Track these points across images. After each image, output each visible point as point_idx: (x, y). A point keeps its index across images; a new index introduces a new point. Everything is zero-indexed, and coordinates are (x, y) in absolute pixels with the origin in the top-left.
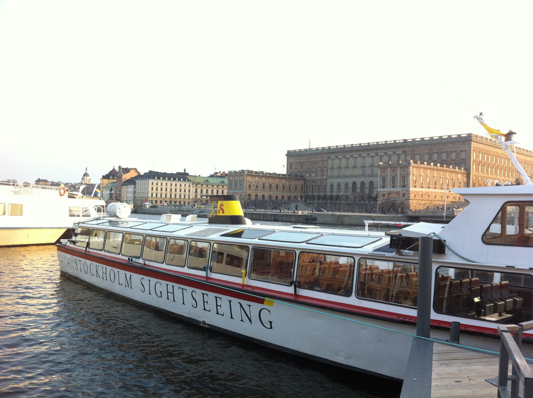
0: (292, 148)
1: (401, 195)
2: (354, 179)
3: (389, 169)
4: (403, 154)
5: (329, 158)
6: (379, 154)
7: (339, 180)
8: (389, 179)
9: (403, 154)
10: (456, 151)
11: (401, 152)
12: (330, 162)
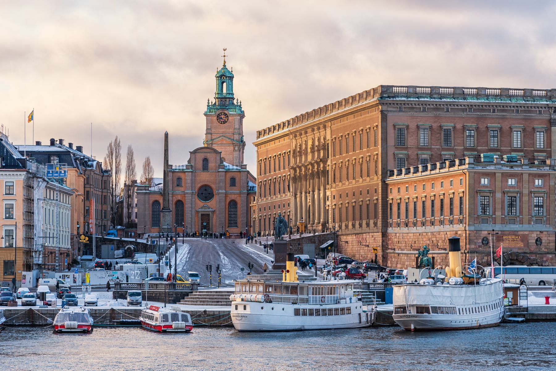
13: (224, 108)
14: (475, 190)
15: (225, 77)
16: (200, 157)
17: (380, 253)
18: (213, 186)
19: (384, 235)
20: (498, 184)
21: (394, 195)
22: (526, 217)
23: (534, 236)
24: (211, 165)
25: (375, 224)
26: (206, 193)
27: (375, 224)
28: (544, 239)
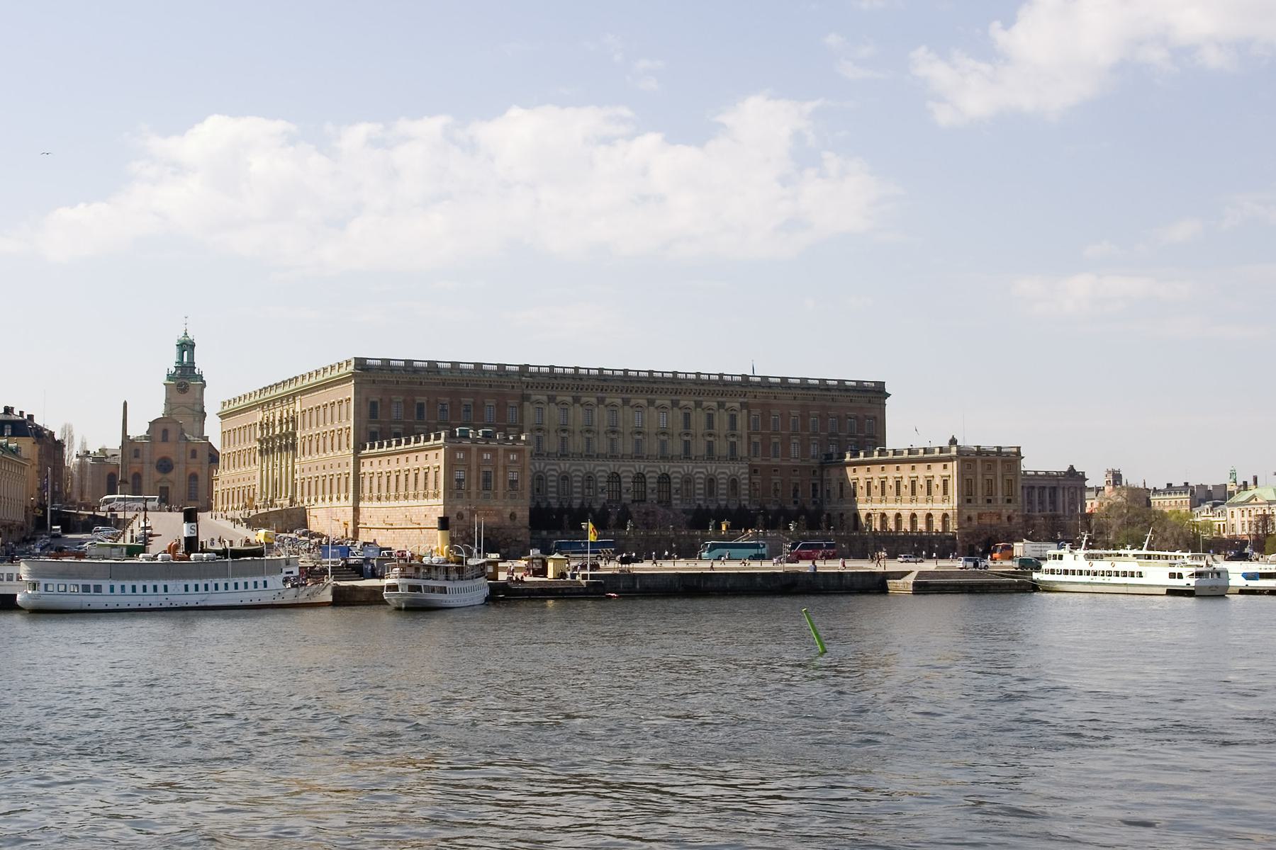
0: (375, 352)
1: (1004, 518)
2: (612, 466)
3: (979, 462)
4: (745, 411)
5: (525, 398)
6: (682, 403)
7: (564, 466)
8: (979, 486)
9: (745, 411)
10: (856, 418)
11: (737, 405)
12: (529, 410)
13: (185, 380)
14: (450, 465)
15: (186, 346)
16: (160, 427)
17: (351, 527)
18: (173, 458)
19: (356, 510)
20: (474, 459)
21: (366, 468)
22: (500, 491)
23: (509, 510)
24: (171, 436)
25: (346, 498)
26: (165, 466)
27: (346, 498)
28: (519, 514)
